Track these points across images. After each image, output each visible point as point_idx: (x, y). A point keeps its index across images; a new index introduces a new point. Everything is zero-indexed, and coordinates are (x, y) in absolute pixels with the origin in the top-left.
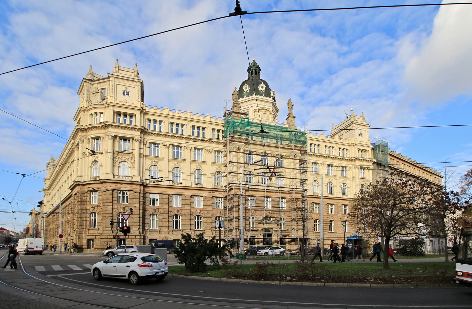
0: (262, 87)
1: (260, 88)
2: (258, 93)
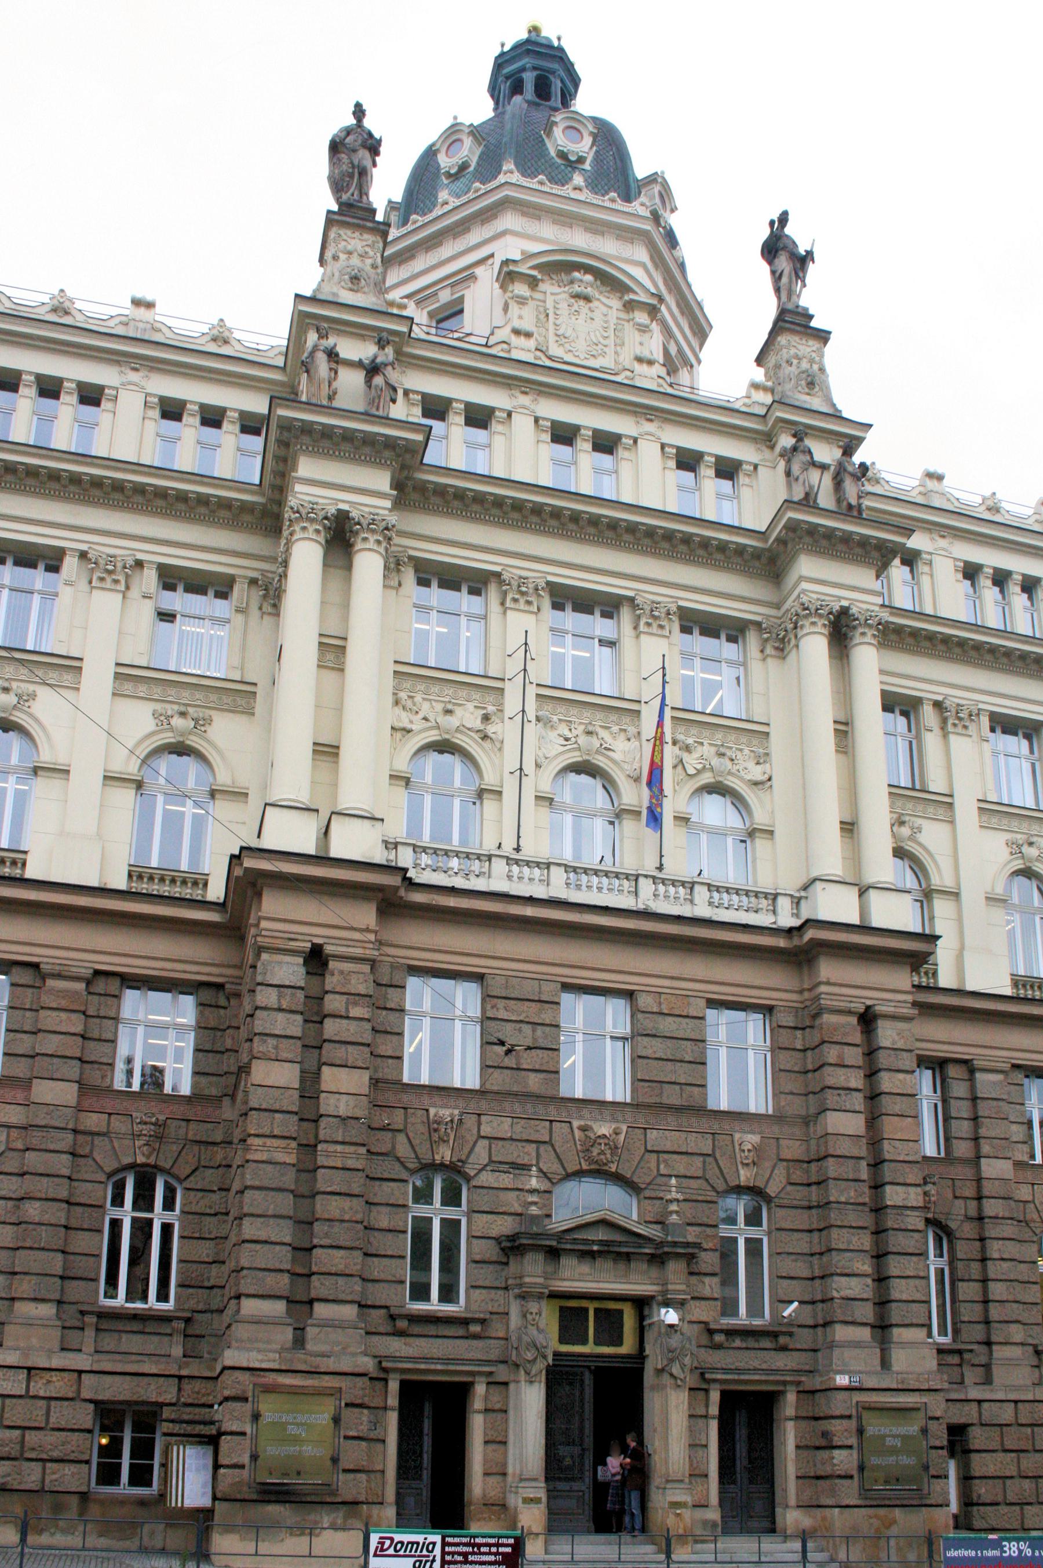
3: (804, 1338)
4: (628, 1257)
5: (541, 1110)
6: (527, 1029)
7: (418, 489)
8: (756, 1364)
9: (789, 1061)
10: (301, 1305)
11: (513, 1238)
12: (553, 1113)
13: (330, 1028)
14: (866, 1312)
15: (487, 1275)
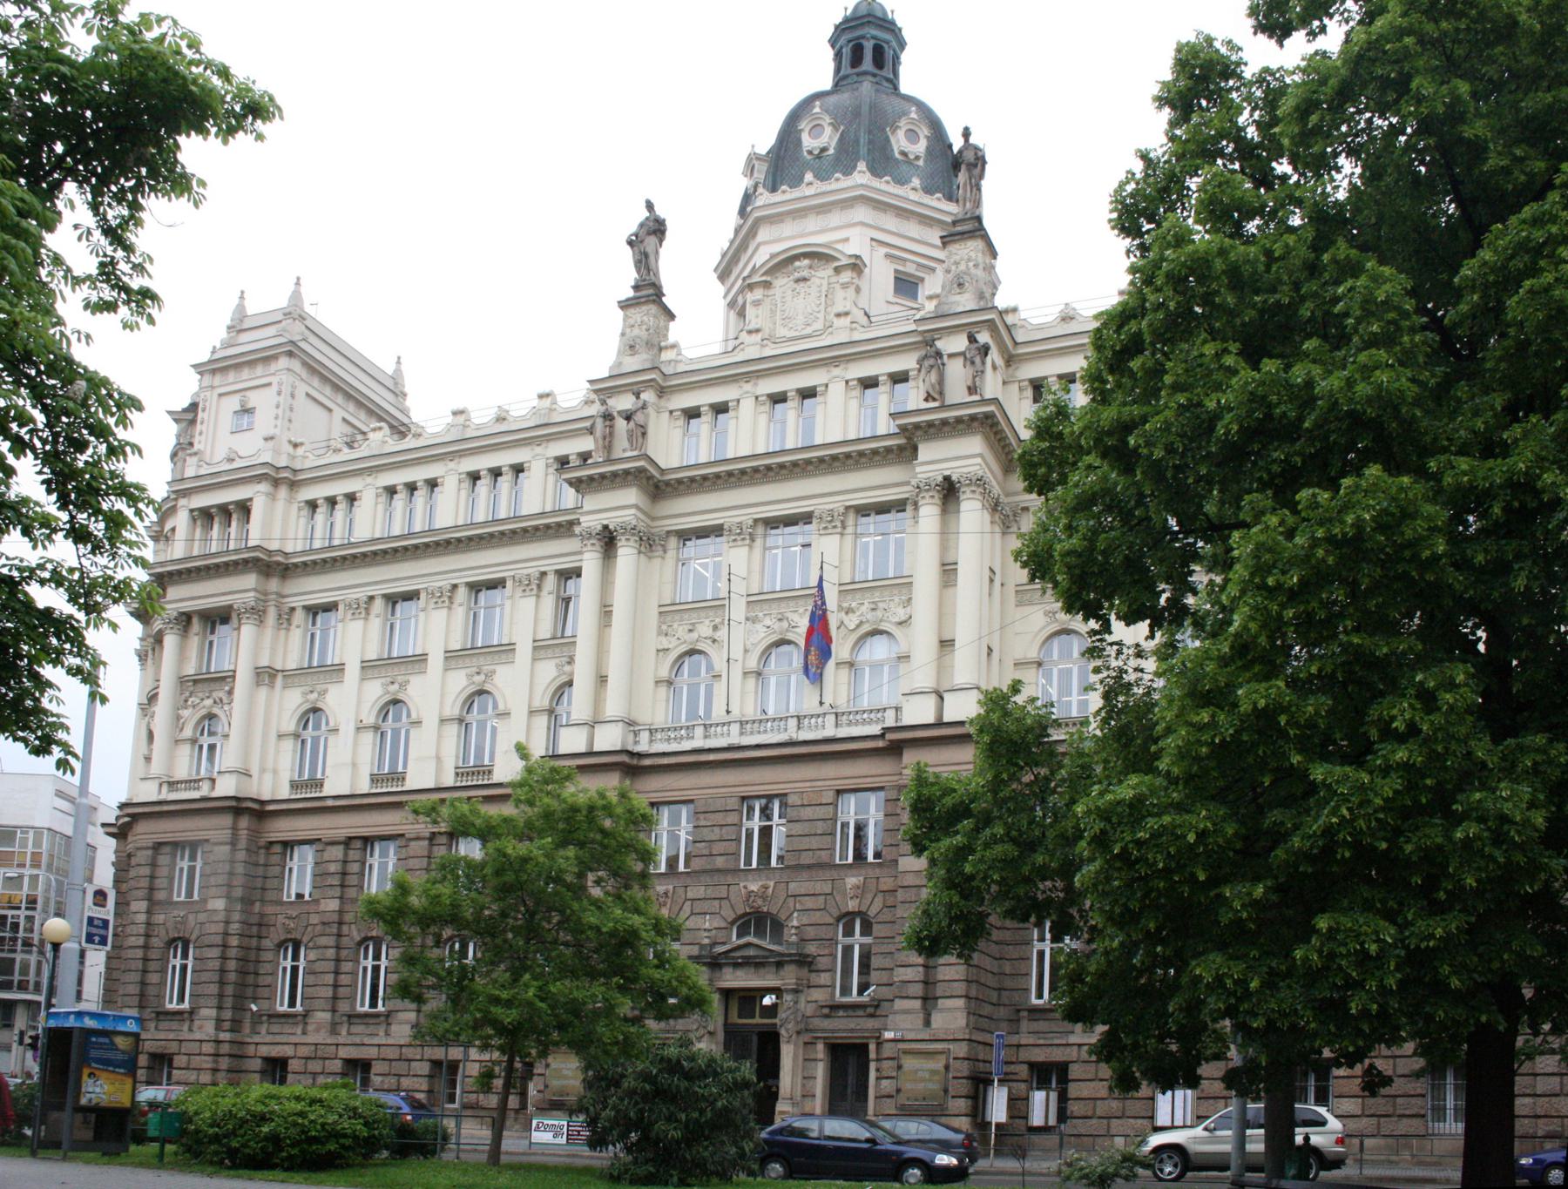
0: (912, 135)
1: (899, 141)
2: (883, 162)
5: (722, 880)
6: (716, 829)
7: (659, 486)
8: (852, 1026)
12: (730, 880)
14: (918, 989)
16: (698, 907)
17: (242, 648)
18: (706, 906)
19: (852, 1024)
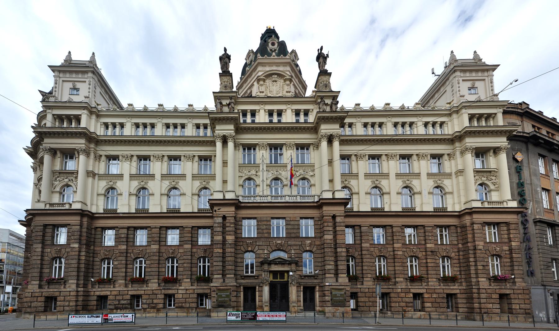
3: (320, 277)
4: (284, 264)
9: (318, 227)
10: (224, 275)
11: (262, 262)
12: (270, 240)
13: (227, 229)
15: (259, 268)
16: (261, 247)
17: (79, 164)
18: (263, 247)
19: (310, 281)
